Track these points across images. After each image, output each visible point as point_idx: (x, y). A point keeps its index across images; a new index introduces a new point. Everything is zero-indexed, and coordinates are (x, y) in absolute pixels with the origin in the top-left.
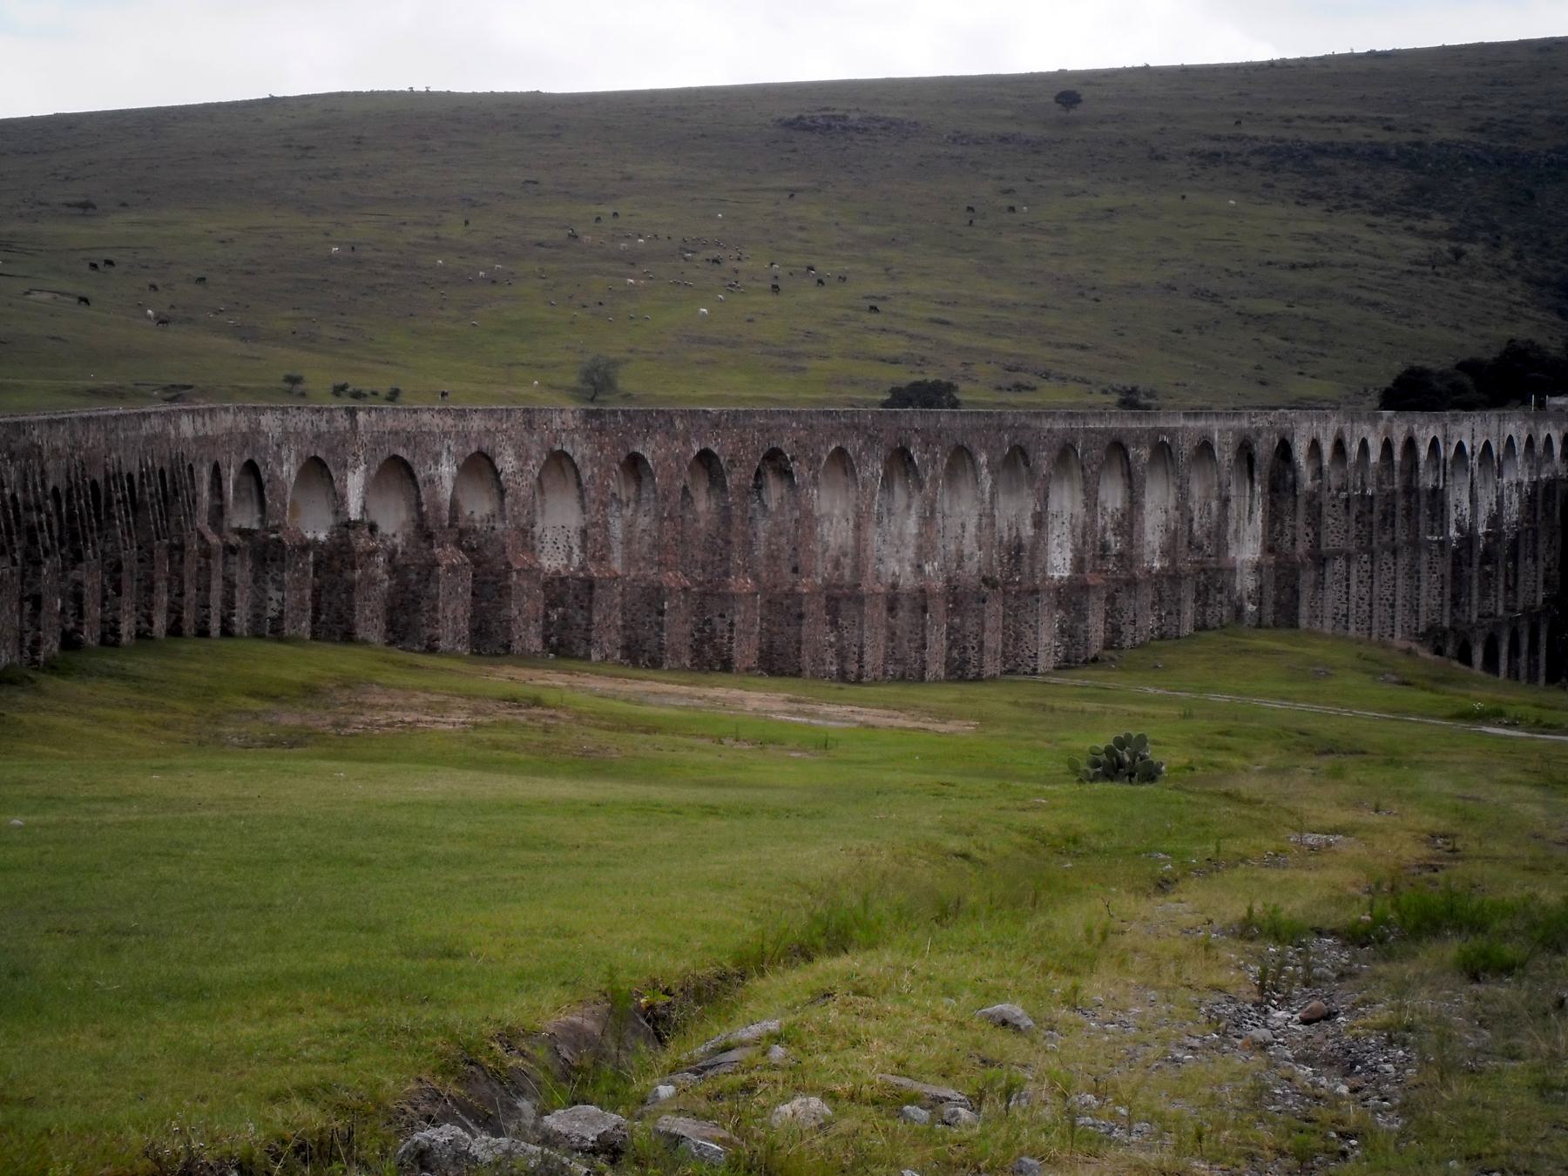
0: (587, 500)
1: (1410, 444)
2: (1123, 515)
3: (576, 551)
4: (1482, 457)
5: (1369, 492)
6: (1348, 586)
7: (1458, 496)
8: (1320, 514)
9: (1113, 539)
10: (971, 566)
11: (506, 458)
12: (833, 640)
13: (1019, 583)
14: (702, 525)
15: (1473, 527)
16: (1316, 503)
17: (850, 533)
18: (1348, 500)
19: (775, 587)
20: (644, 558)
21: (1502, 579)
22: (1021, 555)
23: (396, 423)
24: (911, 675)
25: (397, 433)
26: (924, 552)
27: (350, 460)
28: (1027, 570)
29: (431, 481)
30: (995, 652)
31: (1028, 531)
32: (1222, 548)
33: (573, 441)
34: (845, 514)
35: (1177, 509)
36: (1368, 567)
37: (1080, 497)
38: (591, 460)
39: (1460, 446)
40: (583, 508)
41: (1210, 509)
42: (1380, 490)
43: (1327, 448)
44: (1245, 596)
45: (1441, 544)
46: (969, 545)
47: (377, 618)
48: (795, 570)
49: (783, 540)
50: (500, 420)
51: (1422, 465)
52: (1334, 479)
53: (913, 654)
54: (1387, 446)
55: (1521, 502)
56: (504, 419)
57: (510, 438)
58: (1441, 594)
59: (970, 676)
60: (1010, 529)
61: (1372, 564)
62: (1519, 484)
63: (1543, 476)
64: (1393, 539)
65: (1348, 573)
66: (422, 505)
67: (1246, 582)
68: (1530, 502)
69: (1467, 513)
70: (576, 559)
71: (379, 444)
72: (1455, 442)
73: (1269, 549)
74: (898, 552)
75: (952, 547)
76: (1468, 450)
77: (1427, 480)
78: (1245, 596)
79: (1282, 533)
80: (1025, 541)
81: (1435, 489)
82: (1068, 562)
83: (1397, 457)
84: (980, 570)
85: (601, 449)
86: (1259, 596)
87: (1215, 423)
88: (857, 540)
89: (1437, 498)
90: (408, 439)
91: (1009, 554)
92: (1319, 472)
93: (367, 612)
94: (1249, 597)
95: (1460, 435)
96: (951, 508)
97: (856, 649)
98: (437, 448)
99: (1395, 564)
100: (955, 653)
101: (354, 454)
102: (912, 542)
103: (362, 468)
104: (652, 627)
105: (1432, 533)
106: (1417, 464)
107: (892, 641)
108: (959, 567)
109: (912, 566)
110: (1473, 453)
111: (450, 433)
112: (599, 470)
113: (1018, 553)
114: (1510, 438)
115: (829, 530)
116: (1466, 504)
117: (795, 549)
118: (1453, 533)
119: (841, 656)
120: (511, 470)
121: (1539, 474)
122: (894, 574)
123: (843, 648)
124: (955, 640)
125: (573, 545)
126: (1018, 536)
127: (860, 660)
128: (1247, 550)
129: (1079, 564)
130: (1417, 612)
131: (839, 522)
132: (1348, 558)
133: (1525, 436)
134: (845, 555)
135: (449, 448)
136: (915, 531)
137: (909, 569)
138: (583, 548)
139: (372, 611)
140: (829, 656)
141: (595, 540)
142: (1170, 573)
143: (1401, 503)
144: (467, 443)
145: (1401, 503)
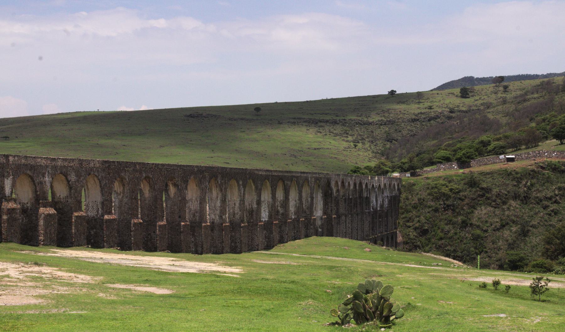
0: (104, 192)
1: (361, 184)
2: (283, 202)
3: (100, 209)
4: (378, 188)
5: (351, 197)
6: (346, 224)
8: (338, 203)
9: (280, 209)
10: (237, 217)
11: (72, 176)
12: (193, 240)
13: (253, 222)
14: (147, 202)
15: (376, 208)
16: (337, 200)
17: (198, 205)
18: (345, 199)
19: (173, 223)
20: (126, 213)
21: (384, 223)
22: (253, 214)
23: (26, 161)
24: (219, 251)
25: (26, 165)
26: (223, 212)
27: (6, 174)
28: (255, 218)
29: (41, 183)
30: (245, 244)
31: (255, 206)
32: (311, 213)
33: (98, 171)
34: (196, 199)
35: (299, 200)
36: (351, 219)
37: (271, 196)
38: (105, 178)
39: (373, 185)
40: (102, 194)
41: (308, 201)
42: (353, 197)
43: (340, 183)
44: (318, 226)
45: (369, 213)
46: (237, 210)
47: (17, 233)
48: (180, 217)
49: (176, 207)
50: (69, 162)
51: (364, 190)
52: (341, 193)
53: (219, 245)
54: (355, 184)
55: (388, 201)
56: (71, 163)
57: (73, 169)
58: (369, 227)
59: (238, 251)
60: (249, 205)
61: (352, 218)
62: (388, 196)
63: (393, 195)
64: (357, 211)
65: (346, 220)
66: (37, 192)
67: (319, 223)
68: (390, 202)
69: (375, 204)
70: (100, 212)
71: (18, 169)
72: (372, 184)
73: (325, 213)
74: (214, 212)
75: (231, 211)
76: (375, 186)
77: (365, 195)
78: (318, 226)
79: (328, 208)
80: (254, 209)
81: (367, 197)
82: (267, 216)
83: (357, 188)
84: (240, 218)
85: (109, 174)
86: (322, 226)
87: (309, 175)
88: (200, 207)
89: (368, 199)
90: (31, 167)
91: (249, 213)
92: (338, 191)
93: (12, 231)
94: (319, 227)
95: (373, 182)
96: (231, 199)
97: (201, 243)
98: (44, 171)
99: (357, 218)
100: (233, 244)
101: (7, 172)
102: (218, 208)
103: (11, 177)
104: (129, 236)
105: (366, 210)
106: (362, 190)
107: (213, 240)
108: (234, 217)
109: (219, 216)
110: (376, 187)
111: (49, 166)
112: (108, 181)
113: (252, 213)
114: (385, 184)
115: (191, 204)
116: (375, 202)
117: (179, 210)
118: (372, 210)
119: (196, 245)
120: (74, 180)
121: (392, 194)
122: (213, 219)
123: (196, 243)
124: (233, 240)
125: (99, 207)
126: (252, 208)
127: (202, 247)
128: (319, 213)
129: (270, 216)
130: (363, 232)
131: (195, 202)
132: (346, 216)
133: (388, 183)
134: (197, 212)
135: (49, 171)
136: (220, 205)
137: (218, 217)
138: (102, 208)
139: (14, 230)
140: (192, 245)
141: (107, 206)
142: (297, 219)
143: (359, 201)
144: (56, 170)
145: (359, 201)
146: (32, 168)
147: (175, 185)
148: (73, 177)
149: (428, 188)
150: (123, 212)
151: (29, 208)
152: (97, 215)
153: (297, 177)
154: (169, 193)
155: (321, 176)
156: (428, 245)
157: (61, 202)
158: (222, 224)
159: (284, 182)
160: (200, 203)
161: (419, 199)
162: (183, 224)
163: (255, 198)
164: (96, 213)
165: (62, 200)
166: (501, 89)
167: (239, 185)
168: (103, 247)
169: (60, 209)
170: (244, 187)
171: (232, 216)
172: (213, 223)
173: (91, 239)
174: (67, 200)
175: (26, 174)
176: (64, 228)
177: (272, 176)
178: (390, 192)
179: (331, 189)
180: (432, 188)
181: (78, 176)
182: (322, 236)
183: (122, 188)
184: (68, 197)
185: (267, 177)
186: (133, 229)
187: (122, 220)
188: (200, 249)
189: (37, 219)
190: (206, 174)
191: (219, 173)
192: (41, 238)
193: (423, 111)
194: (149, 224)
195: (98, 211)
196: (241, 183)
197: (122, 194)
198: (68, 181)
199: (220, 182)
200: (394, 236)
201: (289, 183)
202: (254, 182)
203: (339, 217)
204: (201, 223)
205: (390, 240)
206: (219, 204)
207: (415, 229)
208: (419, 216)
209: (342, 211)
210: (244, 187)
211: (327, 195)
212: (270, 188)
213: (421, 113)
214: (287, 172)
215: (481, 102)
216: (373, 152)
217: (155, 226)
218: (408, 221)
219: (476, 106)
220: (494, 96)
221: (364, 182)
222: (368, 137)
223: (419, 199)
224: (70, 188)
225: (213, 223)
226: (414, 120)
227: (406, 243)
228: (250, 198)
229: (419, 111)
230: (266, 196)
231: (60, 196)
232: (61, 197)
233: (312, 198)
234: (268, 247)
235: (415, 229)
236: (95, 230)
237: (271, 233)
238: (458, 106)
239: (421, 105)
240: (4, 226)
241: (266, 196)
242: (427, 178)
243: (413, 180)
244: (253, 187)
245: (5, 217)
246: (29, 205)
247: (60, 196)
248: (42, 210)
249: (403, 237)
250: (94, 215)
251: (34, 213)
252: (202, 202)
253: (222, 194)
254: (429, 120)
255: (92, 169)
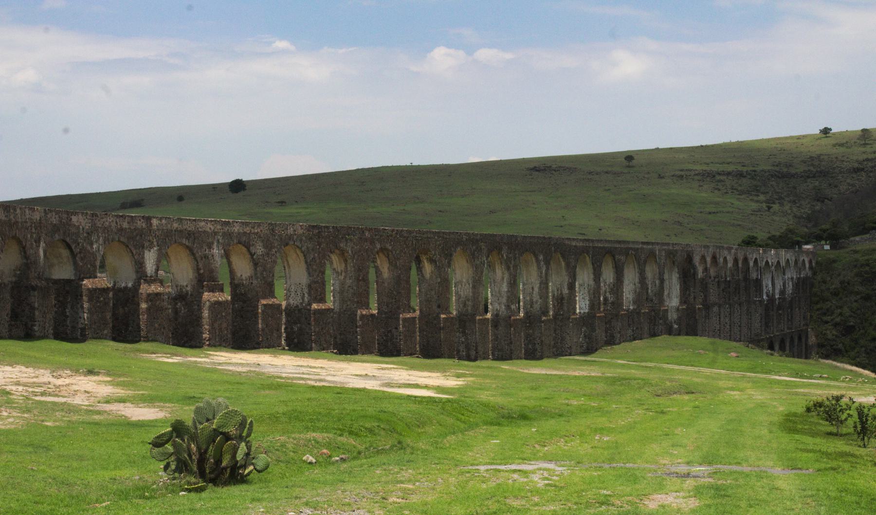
0: (311, 270)
1: (746, 260)
2: (614, 285)
3: (306, 295)
4: (776, 267)
5: (728, 279)
6: (720, 318)
7: (767, 283)
8: (706, 287)
9: (609, 296)
10: (537, 306)
11: (258, 247)
12: (463, 340)
13: (562, 315)
14: (386, 285)
15: (773, 295)
16: (704, 283)
17: (471, 290)
18: (718, 282)
19: (430, 315)
20: (350, 300)
21: (786, 316)
22: (565, 302)
23: (180, 226)
24: (506, 356)
25: (181, 231)
26: (513, 297)
27: (147, 244)
28: (565, 308)
29: (206, 257)
30: (549, 346)
31: (566, 291)
32: (661, 301)
33: (301, 240)
34: (468, 281)
35: (639, 283)
36: (729, 310)
37: (592, 276)
38: (313, 250)
39: (767, 262)
40: (309, 274)
41: (656, 284)
42: (733, 279)
43: (709, 259)
44: (673, 321)
45: (760, 301)
47: (164, 328)
48: (439, 306)
49: (433, 293)
50: (253, 228)
51: (751, 269)
52: (712, 272)
53: (506, 347)
54: (736, 261)
55: (793, 286)
56: (256, 228)
57: (260, 237)
58: (761, 322)
59: (537, 357)
60: (558, 290)
61: (730, 308)
62: (792, 278)
63: (802, 276)
64: (739, 299)
65: (720, 312)
66: (200, 269)
67: (673, 316)
69: (771, 289)
70: (306, 299)
71: (168, 236)
72: (765, 260)
74: (498, 299)
75: (528, 298)
76: (770, 264)
78: (673, 321)
79: (689, 295)
80: (565, 296)
81: (757, 279)
82: (587, 305)
83: (740, 265)
84: (540, 308)
85: (319, 244)
86: (679, 321)
87: (657, 246)
88: (474, 293)
89: (758, 283)
90: (189, 235)
91: (558, 301)
92: (706, 270)
93: (156, 325)
94: (675, 322)
95: (767, 258)
96: (527, 280)
97: (474, 344)
98: (210, 240)
99: (740, 309)
100: (530, 346)
101: (149, 241)
103: (155, 248)
104: (353, 333)
105: (756, 297)
106: (749, 268)
107: (497, 341)
108: (531, 307)
109: (505, 306)
110: (772, 265)
111: (219, 233)
112: (318, 255)
113: (562, 301)
114: (788, 260)
115: (461, 289)
116: (770, 286)
117: (438, 297)
118: (765, 297)
119: (468, 348)
120: (261, 253)
121: (800, 275)
122: (497, 310)
123: (468, 344)
124: (530, 340)
125: (305, 292)
126: (561, 293)
127: (476, 350)
128: (673, 301)
130: (750, 329)
131: (465, 285)
132: (720, 306)
133: (794, 259)
134: (468, 300)
135: (218, 240)
136: (506, 290)
137: (504, 307)
138: (309, 294)
139: (159, 325)
141: (317, 290)
142: (637, 311)
143: (743, 284)
144: (231, 238)
145: (743, 284)
146: (190, 235)
147: (432, 261)
148: (259, 249)
149: (855, 266)
150: (346, 299)
151: (190, 293)
152: (301, 304)
153: (637, 250)
154: (423, 271)
155: (677, 248)
156: (854, 348)
157: (243, 285)
158: (510, 317)
159: (613, 256)
160: (474, 287)
161: (842, 282)
162: (443, 316)
163: (566, 279)
164: (301, 301)
165: (244, 282)
167: (538, 261)
168: (311, 349)
169: (242, 294)
170: (547, 263)
171: (529, 306)
172: (497, 315)
173: (295, 338)
174: (251, 281)
175: (181, 244)
176: (248, 322)
177: (594, 247)
178: (797, 272)
179: (695, 268)
180: (862, 266)
181: (268, 246)
182: (679, 334)
183: (343, 265)
184: (252, 277)
185: (584, 250)
186: (360, 323)
187: (345, 311)
188: (473, 353)
189: (200, 309)
190: (483, 245)
191: (505, 243)
192: (206, 336)
194: (388, 315)
195: (303, 298)
196: (541, 257)
197: (343, 274)
198: (252, 255)
199: (507, 256)
200: (802, 336)
201: (623, 258)
202: (563, 256)
203: (707, 307)
204: (474, 315)
205: (796, 341)
206: (505, 288)
207: (836, 325)
208: (841, 307)
209: (713, 298)
210: (547, 263)
211: (687, 275)
212: (590, 266)
214: (619, 242)
217: (398, 319)
218: (825, 314)
221: (752, 257)
223: (842, 282)
224: (256, 264)
225: (497, 315)
227: (820, 346)
228: (557, 281)
230: (585, 277)
231: (241, 275)
232: (244, 277)
233: (662, 281)
234: (589, 350)
235: (836, 325)
236: (299, 325)
237: (594, 330)
240: (143, 318)
241: (585, 277)
242: (856, 252)
243: (833, 255)
244: (563, 264)
245: (144, 306)
246: (189, 289)
247: (241, 275)
248: (206, 295)
249: (816, 336)
250: (298, 304)
251: (196, 301)
252: (477, 283)
253: (510, 274)
255: (290, 237)
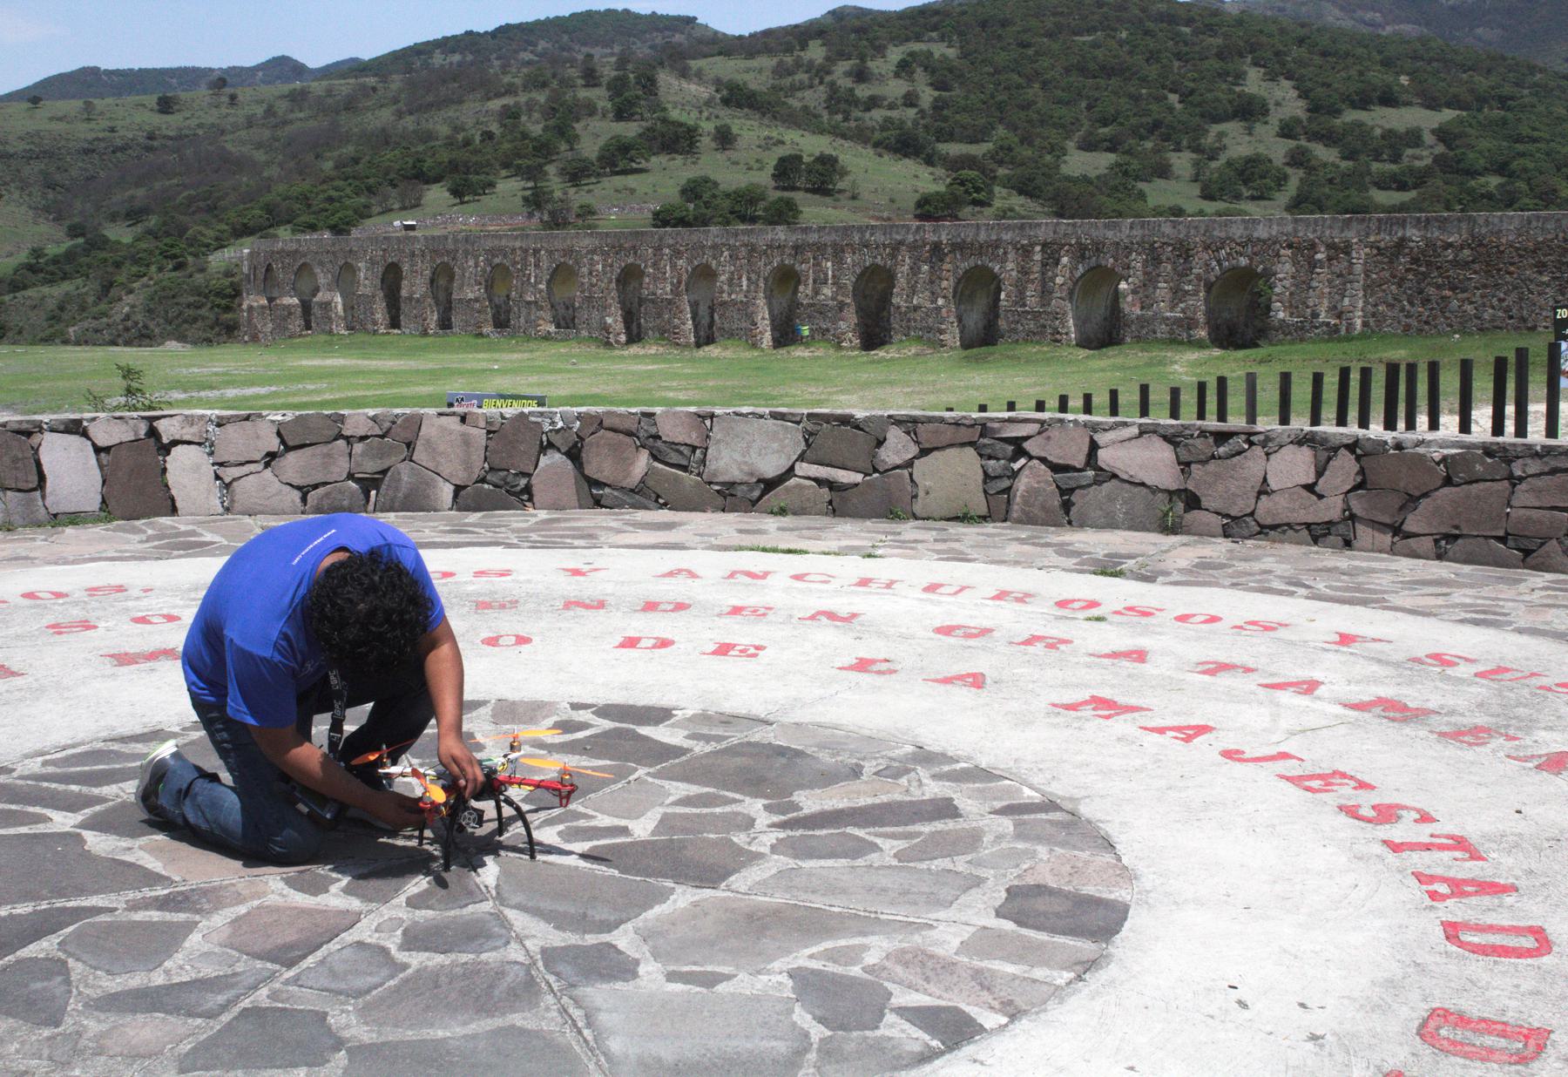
166: (225, 99)
193: (101, 135)
213: (98, 139)
215: (197, 122)
216: (30, 207)
219: (189, 128)
220: (214, 112)
222: (13, 181)
226: (87, 152)
229: (94, 135)
238: (159, 129)
239: (92, 125)
254: (114, 152)
